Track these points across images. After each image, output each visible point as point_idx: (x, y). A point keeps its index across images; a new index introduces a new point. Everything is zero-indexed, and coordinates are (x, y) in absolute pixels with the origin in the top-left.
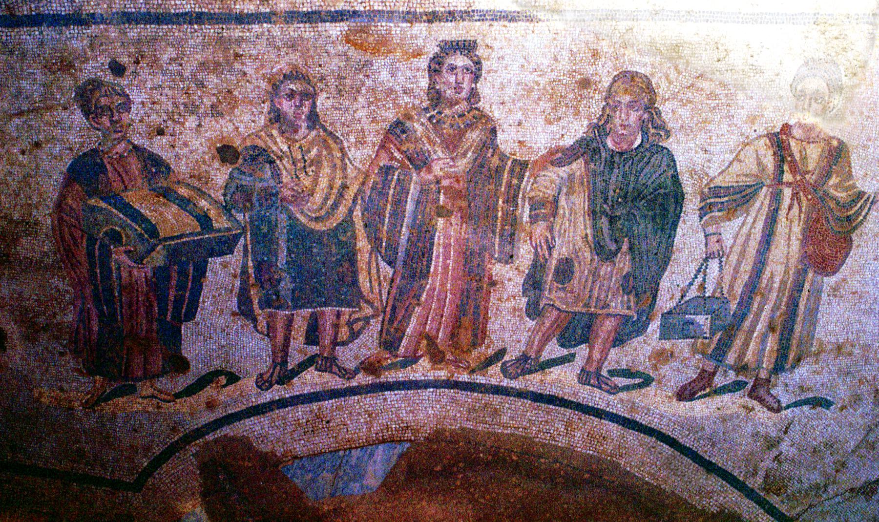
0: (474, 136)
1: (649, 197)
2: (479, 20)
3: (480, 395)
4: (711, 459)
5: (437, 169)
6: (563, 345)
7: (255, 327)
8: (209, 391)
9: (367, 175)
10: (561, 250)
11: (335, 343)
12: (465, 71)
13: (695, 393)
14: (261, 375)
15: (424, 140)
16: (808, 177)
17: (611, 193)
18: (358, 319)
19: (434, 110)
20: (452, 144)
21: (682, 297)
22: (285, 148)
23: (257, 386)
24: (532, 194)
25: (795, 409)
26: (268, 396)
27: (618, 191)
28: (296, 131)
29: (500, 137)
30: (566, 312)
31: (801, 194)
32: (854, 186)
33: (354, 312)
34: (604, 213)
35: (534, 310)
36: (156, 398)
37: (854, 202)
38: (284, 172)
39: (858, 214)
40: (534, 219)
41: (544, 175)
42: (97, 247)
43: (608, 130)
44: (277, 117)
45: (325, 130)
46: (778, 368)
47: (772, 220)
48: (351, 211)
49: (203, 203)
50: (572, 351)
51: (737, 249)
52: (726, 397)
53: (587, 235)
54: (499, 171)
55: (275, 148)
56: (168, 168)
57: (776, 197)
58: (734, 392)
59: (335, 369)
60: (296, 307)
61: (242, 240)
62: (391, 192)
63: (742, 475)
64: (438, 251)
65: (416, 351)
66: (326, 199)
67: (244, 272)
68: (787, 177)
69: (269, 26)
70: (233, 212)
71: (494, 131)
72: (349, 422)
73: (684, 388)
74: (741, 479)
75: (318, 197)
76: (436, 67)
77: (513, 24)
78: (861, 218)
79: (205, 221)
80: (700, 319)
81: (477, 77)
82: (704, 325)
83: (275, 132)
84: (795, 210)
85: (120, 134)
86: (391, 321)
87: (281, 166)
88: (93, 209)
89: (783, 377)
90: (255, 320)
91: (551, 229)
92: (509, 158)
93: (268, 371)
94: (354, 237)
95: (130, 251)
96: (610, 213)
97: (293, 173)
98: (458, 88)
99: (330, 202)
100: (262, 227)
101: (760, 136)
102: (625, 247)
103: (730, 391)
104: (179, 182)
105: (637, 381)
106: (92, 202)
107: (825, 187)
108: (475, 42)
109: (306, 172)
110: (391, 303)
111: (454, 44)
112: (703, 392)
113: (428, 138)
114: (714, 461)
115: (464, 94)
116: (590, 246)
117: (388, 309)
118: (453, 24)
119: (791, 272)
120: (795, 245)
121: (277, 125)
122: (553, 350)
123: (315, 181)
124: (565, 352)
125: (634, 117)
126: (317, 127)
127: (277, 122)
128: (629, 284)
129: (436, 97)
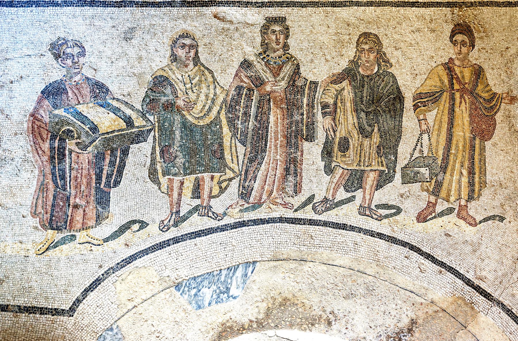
1: (386, 100)
2: (286, 7)
3: (301, 226)
4: (442, 260)
5: (268, 88)
6: (347, 191)
7: (160, 188)
8: (128, 234)
9: (228, 92)
10: (341, 133)
11: (211, 197)
12: (280, 33)
13: (427, 217)
14: (163, 221)
15: (261, 71)
16: (466, 86)
17: (365, 98)
18: (225, 180)
19: (265, 54)
20: (276, 75)
21: (412, 157)
22: (180, 78)
23: (160, 229)
24: (322, 101)
25: (484, 223)
27: (368, 97)
29: (302, 70)
30: (348, 170)
31: (464, 95)
33: (221, 176)
35: (329, 170)
36: (89, 243)
37: (492, 99)
38: (179, 91)
40: (324, 114)
41: (327, 89)
42: (57, 141)
43: (359, 64)
44: (174, 58)
45: (204, 66)
46: (470, 198)
47: (452, 111)
48: (219, 113)
49: (128, 112)
50: (353, 194)
51: (436, 127)
52: (445, 218)
53: (354, 123)
54: (303, 88)
55: (174, 77)
56: (108, 90)
57: (452, 98)
58: (448, 214)
59: (210, 214)
61: (152, 133)
62: (242, 101)
63: (462, 270)
64: (271, 136)
65: (261, 198)
66: (204, 106)
67: (153, 153)
68: (456, 86)
69: (171, 8)
70: (147, 115)
71: (298, 65)
72: (219, 250)
73: (419, 215)
74: (461, 272)
75: (199, 106)
76: (265, 29)
77: (304, 9)
78: (498, 107)
79: (129, 122)
80: (423, 170)
81: (287, 36)
82: (425, 174)
83: (174, 68)
85: (77, 70)
87: (177, 88)
88: (56, 116)
89: (473, 203)
90: (159, 184)
92: (307, 80)
93: (167, 218)
94: (221, 127)
95: (79, 143)
96: (365, 110)
97: (184, 91)
98: (278, 43)
99: (207, 108)
100: (165, 124)
101: (439, 65)
104: (114, 98)
105: (393, 211)
106: (56, 112)
107: (476, 91)
109: (192, 90)
110: (244, 168)
111: (274, 19)
112: (431, 216)
113: (263, 70)
114: (444, 262)
116: (357, 130)
117: (243, 173)
118: (273, 8)
119: (468, 141)
120: (466, 123)
121: (174, 64)
122: (342, 194)
123: (198, 96)
124: (349, 195)
125: (372, 56)
126: (199, 64)
127: (175, 62)
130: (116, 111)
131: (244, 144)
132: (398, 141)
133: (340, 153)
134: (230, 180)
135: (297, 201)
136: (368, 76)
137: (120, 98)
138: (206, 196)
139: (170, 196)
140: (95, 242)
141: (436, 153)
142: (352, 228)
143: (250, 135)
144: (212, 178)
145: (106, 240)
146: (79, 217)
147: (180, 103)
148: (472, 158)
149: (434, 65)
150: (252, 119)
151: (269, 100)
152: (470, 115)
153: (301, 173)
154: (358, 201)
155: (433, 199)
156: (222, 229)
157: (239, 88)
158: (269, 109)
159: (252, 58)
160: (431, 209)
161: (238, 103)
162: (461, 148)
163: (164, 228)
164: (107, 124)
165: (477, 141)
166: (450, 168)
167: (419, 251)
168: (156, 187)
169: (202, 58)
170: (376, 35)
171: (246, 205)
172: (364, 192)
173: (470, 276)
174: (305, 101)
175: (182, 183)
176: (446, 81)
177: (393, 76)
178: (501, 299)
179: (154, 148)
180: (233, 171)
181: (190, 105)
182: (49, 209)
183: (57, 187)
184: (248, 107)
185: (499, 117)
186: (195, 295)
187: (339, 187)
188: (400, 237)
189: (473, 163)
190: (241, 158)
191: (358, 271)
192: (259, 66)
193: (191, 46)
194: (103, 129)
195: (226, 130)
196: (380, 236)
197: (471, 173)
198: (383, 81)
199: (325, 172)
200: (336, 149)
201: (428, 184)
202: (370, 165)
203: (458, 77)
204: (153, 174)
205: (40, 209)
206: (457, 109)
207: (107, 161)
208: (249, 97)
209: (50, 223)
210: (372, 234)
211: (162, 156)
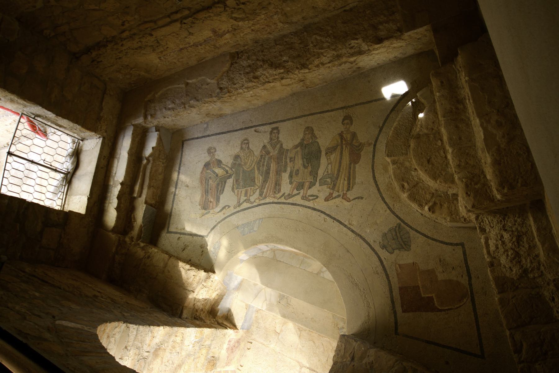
0: (278, 146)
5: (271, 154)
6: (297, 190)
7: (235, 194)
8: (224, 210)
11: (250, 196)
17: (306, 153)
20: (274, 149)
21: (324, 174)
22: (243, 155)
26: (236, 210)
28: (245, 150)
29: (283, 145)
32: (359, 142)
34: (305, 158)
35: (291, 183)
39: (361, 148)
40: (290, 161)
44: (242, 148)
45: (250, 149)
47: (341, 153)
48: (254, 166)
49: (227, 169)
50: (300, 191)
52: (337, 199)
56: (222, 162)
57: (342, 148)
60: (243, 188)
67: (233, 182)
68: (344, 142)
71: (282, 144)
73: (326, 198)
76: (271, 133)
79: (227, 172)
83: (241, 152)
84: (347, 149)
86: (261, 189)
89: (349, 192)
91: (294, 163)
102: (310, 165)
103: (337, 198)
106: (207, 171)
108: (278, 127)
115: (276, 138)
120: (348, 158)
122: (295, 192)
124: (298, 192)
125: (310, 136)
128: (311, 173)
129: (271, 139)
130: (223, 168)
131: (262, 176)
132: (318, 169)
133: (295, 176)
134: (257, 189)
135: (278, 196)
136: (307, 144)
137: (225, 164)
138: (248, 196)
139: (238, 196)
140: (215, 213)
141: (334, 172)
142: (298, 205)
143: (264, 173)
144: (251, 189)
145: (218, 212)
146: (211, 205)
147: (243, 164)
148: (349, 173)
149: (335, 135)
150: (265, 166)
151: (271, 159)
152: (349, 154)
153: (281, 185)
154: (301, 194)
155: (332, 191)
156: (253, 207)
157: (262, 156)
158: (271, 162)
159: (266, 144)
160: (331, 196)
161: (261, 161)
162: (345, 168)
163: (235, 208)
164: (221, 173)
165: (352, 165)
166: (339, 177)
167: (324, 213)
168: (233, 193)
169: (250, 146)
170: (311, 127)
171: (261, 198)
172: (304, 190)
173: (346, 223)
174: (284, 157)
175: (241, 192)
176: (340, 141)
177: (318, 143)
178: (360, 233)
179: (234, 180)
180: (257, 185)
181: (245, 164)
182: (203, 202)
183: (206, 195)
184: (264, 162)
185: (362, 153)
186: (243, 230)
187: (294, 189)
188: (317, 207)
189: (350, 175)
190: (261, 181)
191: (300, 221)
192: (269, 147)
193: (247, 143)
194: (219, 176)
195: (256, 171)
196: (309, 207)
197: (349, 179)
198: (313, 145)
199: (290, 184)
200: (294, 174)
201: (330, 185)
202: (306, 179)
203: (345, 139)
204: (233, 189)
205: (201, 203)
206: (344, 152)
207: (220, 186)
208: (264, 159)
209: (204, 208)
210: (306, 207)
211: (236, 183)
